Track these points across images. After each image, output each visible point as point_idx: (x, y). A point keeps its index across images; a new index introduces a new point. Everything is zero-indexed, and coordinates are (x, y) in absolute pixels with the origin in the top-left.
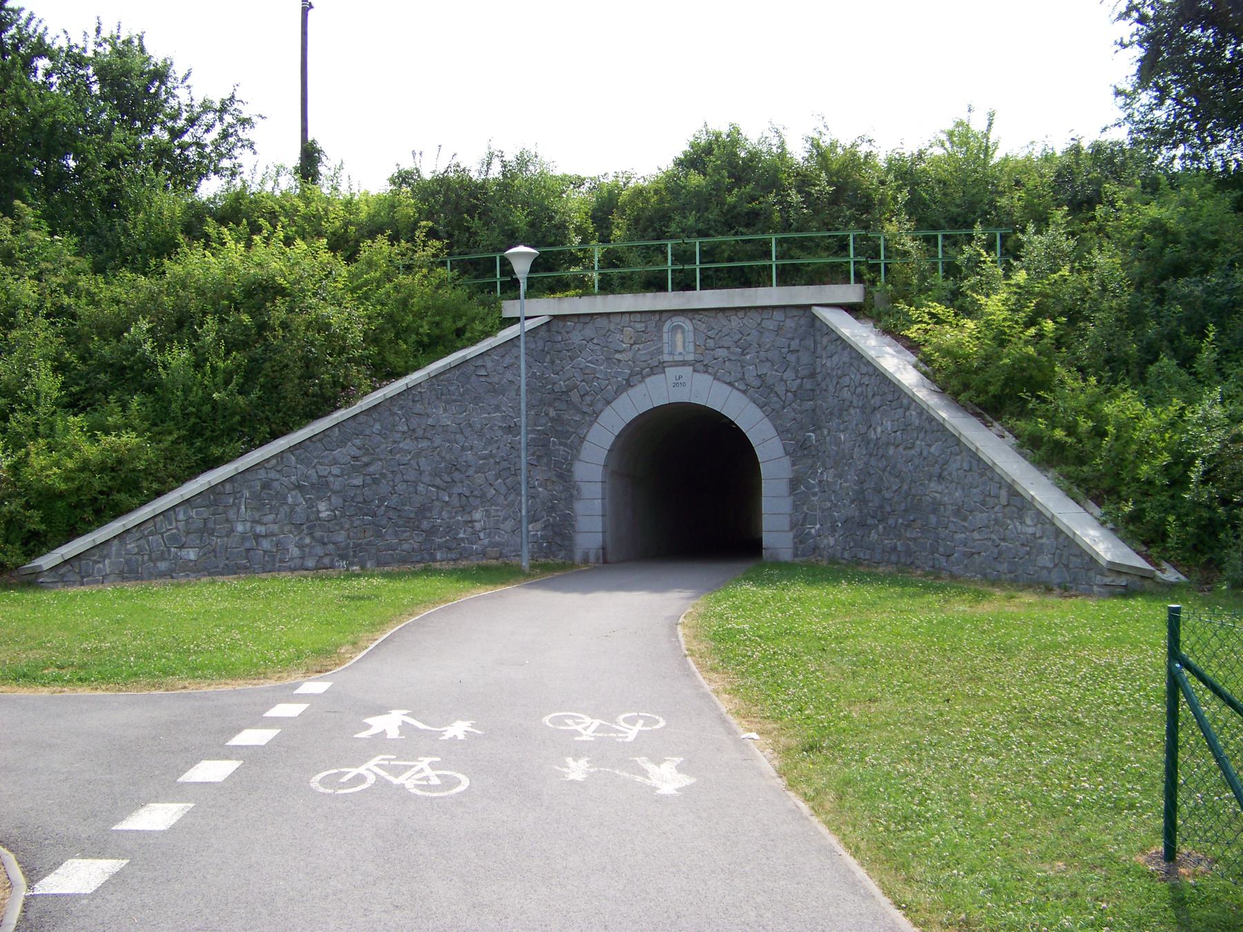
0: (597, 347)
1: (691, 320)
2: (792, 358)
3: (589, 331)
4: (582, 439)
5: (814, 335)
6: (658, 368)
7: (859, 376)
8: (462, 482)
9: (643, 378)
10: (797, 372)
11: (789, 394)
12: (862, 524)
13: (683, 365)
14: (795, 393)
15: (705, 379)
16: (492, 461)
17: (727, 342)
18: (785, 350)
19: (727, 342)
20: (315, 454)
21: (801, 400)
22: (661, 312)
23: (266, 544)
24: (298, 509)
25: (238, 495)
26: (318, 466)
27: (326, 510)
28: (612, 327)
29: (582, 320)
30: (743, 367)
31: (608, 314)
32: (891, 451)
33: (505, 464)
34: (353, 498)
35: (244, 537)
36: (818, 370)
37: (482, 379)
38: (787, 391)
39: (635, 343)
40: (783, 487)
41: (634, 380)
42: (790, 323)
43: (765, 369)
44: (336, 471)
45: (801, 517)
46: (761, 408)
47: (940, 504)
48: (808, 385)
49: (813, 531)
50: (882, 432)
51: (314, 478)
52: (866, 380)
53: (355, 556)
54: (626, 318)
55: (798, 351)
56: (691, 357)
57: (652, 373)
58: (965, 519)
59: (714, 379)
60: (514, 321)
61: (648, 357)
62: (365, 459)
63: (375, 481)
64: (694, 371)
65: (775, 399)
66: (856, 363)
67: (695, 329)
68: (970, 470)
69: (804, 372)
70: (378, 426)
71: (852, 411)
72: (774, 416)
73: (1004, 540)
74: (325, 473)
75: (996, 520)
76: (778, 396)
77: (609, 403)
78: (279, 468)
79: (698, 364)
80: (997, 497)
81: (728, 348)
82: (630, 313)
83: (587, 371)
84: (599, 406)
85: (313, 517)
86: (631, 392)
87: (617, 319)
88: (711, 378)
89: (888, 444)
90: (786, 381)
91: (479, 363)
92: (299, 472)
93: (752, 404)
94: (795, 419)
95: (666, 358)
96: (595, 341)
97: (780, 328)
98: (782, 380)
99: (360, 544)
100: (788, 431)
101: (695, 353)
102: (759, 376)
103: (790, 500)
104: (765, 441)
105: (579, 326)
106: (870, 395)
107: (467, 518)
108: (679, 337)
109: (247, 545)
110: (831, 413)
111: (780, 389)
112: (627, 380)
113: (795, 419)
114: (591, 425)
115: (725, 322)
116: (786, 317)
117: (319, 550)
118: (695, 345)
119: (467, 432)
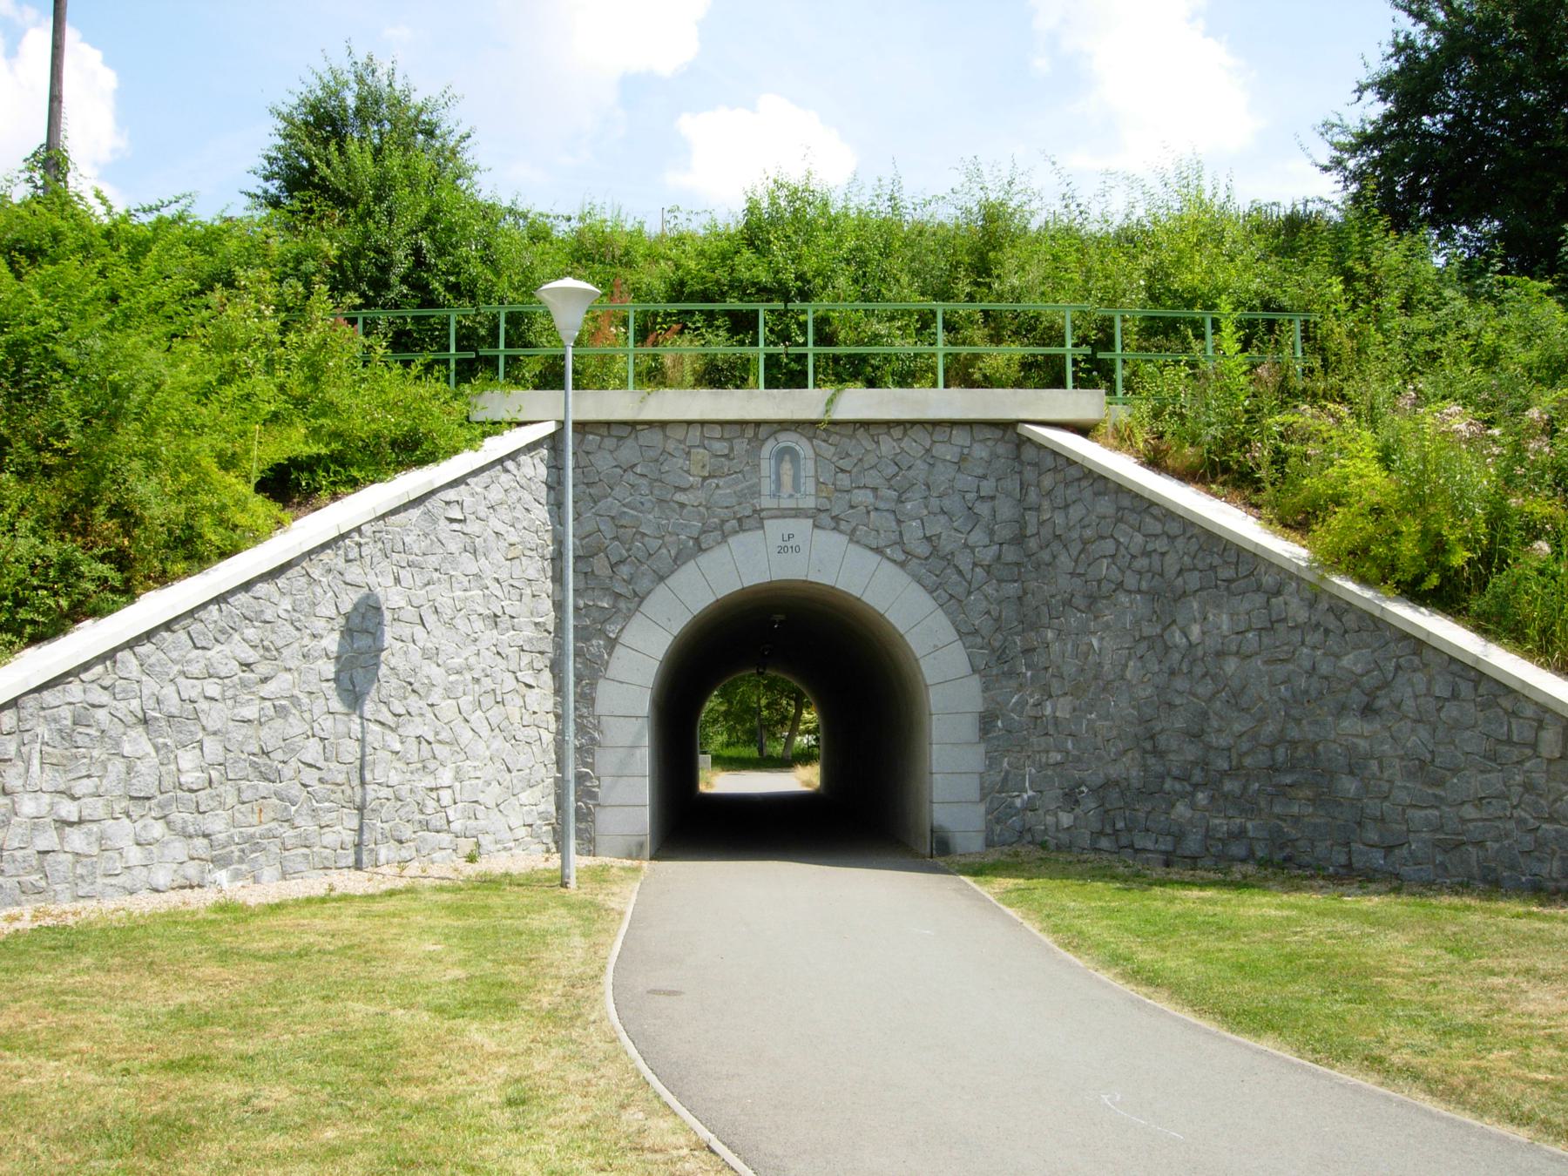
0: (644, 481)
1: (810, 439)
2: (983, 509)
3: (628, 452)
4: (612, 644)
5: (1020, 473)
6: (752, 520)
7: (1139, 538)
8: (422, 715)
9: (725, 537)
10: (992, 533)
11: (978, 570)
12: (1145, 793)
13: (796, 516)
14: (988, 569)
15: (831, 542)
16: (468, 676)
17: (872, 478)
18: (971, 496)
19: (872, 478)
20: (175, 655)
21: (1000, 581)
22: (758, 424)
23: (77, 840)
24: (141, 767)
25: (27, 737)
26: (181, 680)
27: (194, 769)
28: (671, 446)
29: (615, 431)
30: (899, 522)
31: (663, 424)
32: (1231, 665)
33: (487, 683)
34: (242, 743)
35: (36, 823)
36: (1031, 530)
37: (456, 526)
38: (975, 565)
39: (711, 476)
40: (968, 728)
41: (706, 541)
42: (980, 452)
43: (937, 526)
44: (213, 689)
45: (999, 779)
46: (931, 592)
47: (1370, 756)
48: (1010, 554)
49: (1018, 802)
50: (1204, 633)
51: (172, 704)
52: (1161, 545)
53: (241, 860)
54: (695, 433)
55: (993, 498)
56: (810, 503)
57: (741, 528)
58: (1439, 783)
59: (851, 540)
60: (495, 427)
61: (734, 501)
62: (263, 669)
63: (281, 712)
64: (816, 526)
65: (955, 577)
66: (1132, 518)
67: (817, 455)
68: (1455, 696)
69: (1005, 533)
70: (286, 604)
71: (1123, 598)
72: (952, 604)
73: (1551, 819)
74: (194, 694)
75: (1528, 787)
76: (960, 572)
77: (662, 579)
78: (107, 683)
79: (823, 515)
80: (1534, 746)
81: (875, 489)
82: (703, 423)
83: (623, 522)
84: (643, 584)
85: (168, 782)
86: (703, 559)
87: (679, 433)
88: (844, 539)
89: (1220, 654)
90: (972, 549)
91: (451, 495)
92: (146, 692)
93: (915, 585)
94: (988, 613)
95: (766, 502)
96: (638, 470)
97: (963, 458)
98: (966, 545)
99: (252, 836)
100: (976, 632)
101: (817, 496)
102: (929, 539)
103: (982, 748)
104: (936, 648)
105: (610, 443)
106: (1171, 571)
107: (429, 781)
108: (787, 467)
109: (42, 845)
110: (1068, 603)
111: (964, 561)
112: (697, 540)
113: (988, 613)
114: (628, 618)
115: (871, 446)
116: (973, 438)
117: (179, 849)
118: (818, 482)
119: (430, 619)
